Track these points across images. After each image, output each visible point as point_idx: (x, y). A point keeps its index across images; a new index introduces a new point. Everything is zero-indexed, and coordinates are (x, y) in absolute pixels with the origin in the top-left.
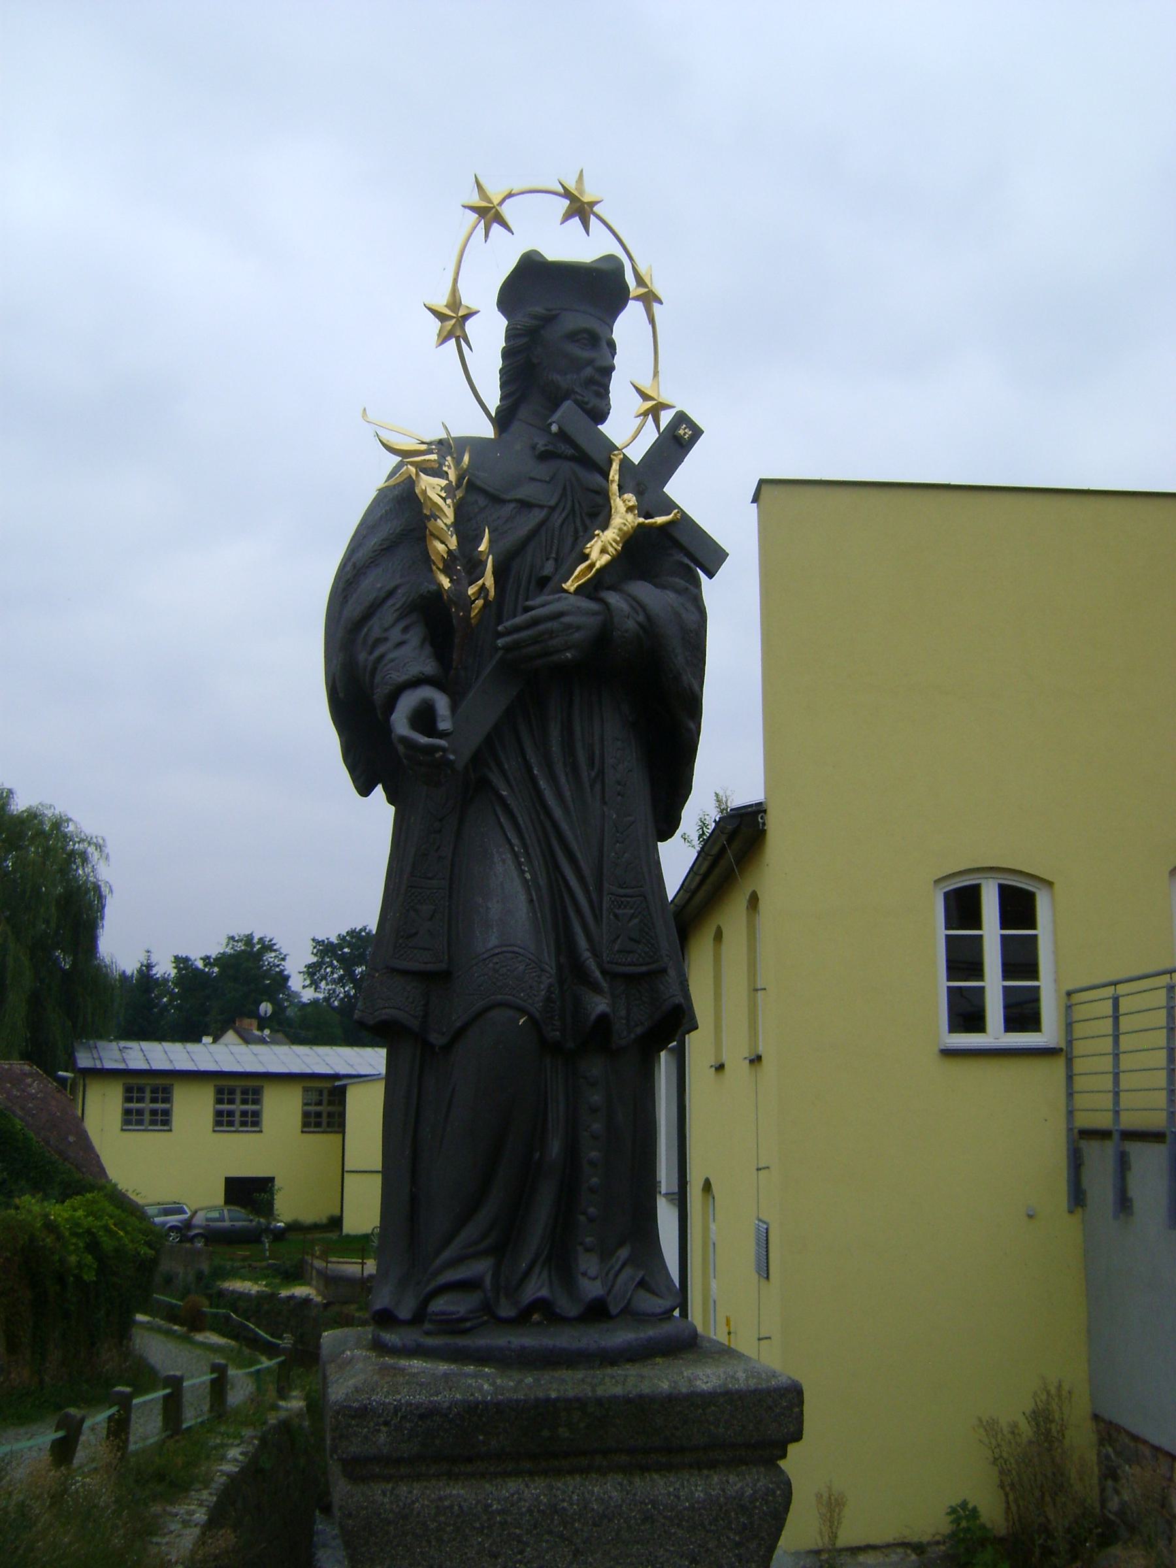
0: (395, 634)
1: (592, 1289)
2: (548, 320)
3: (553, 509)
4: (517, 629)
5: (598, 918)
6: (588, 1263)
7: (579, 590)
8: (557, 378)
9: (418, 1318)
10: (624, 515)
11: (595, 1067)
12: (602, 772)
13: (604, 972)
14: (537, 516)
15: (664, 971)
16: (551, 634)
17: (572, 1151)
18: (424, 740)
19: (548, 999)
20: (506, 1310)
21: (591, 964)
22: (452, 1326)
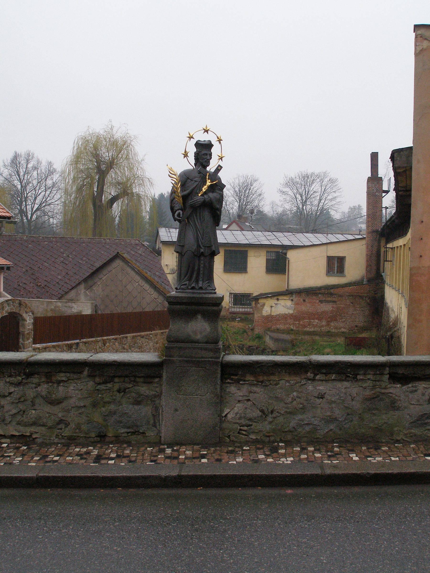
1: (200, 285)
5: (203, 239)
6: (201, 283)
10: (208, 183)
13: (203, 246)
14: (197, 183)
15: (212, 246)
17: (199, 269)
19: (195, 250)
21: (201, 245)
22: (183, 289)
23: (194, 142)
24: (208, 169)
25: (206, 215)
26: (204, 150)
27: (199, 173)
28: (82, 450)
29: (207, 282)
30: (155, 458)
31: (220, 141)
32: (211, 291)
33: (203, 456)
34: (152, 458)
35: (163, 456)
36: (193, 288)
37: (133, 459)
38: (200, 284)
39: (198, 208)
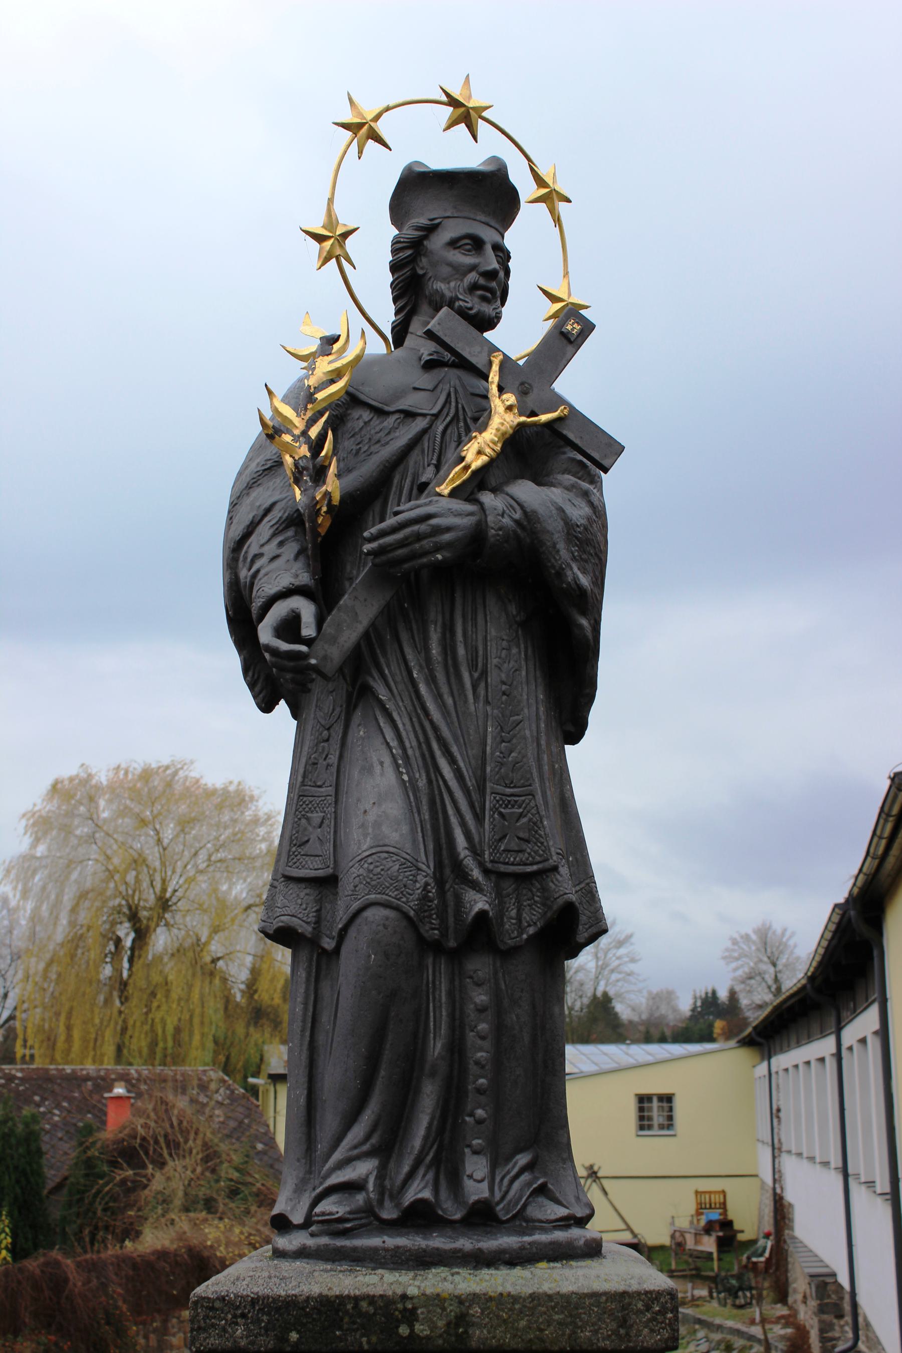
0: (271, 549)
1: (476, 1190)
2: (431, 229)
3: (436, 416)
4: (383, 534)
5: (479, 818)
6: (476, 1167)
7: (454, 494)
10: (503, 416)
11: (480, 966)
12: (484, 673)
13: (486, 872)
14: (420, 424)
15: (555, 869)
16: (419, 537)
17: (457, 1048)
18: (285, 646)
19: (425, 898)
20: (389, 1213)
21: (469, 862)
22: (335, 1227)
25: (494, 637)
26: (453, 227)
29: (523, 1159)
32: (559, 1235)
36: (420, 1217)
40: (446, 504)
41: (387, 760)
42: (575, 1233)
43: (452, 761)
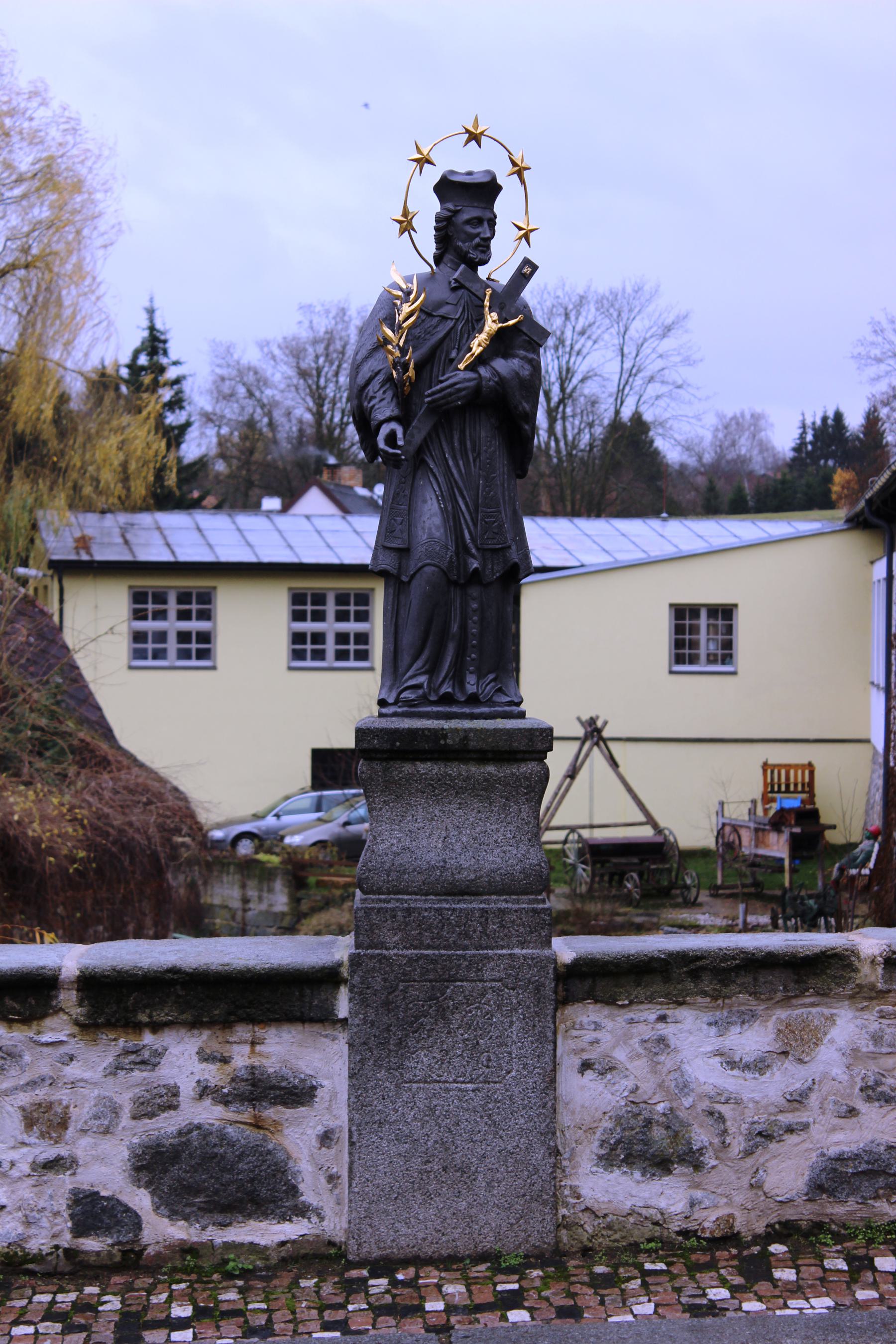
0: (380, 394)
1: (471, 689)
2: (456, 213)
3: (457, 320)
4: (433, 394)
5: (475, 525)
6: (471, 679)
7: (466, 368)
8: (460, 244)
9: (396, 703)
10: (491, 323)
11: (474, 591)
12: (479, 454)
13: (478, 549)
14: (450, 324)
15: (509, 547)
16: (450, 394)
17: (463, 627)
18: (391, 451)
19: (451, 562)
21: (471, 546)
22: (409, 703)
23: (433, 175)
24: (483, 272)
26: (467, 205)
27: (454, 289)
28: (60, 1297)
29: (491, 676)
30: (340, 1315)
31: (519, 172)
32: (507, 708)
33: (513, 1300)
34: (328, 1315)
35: (365, 1306)
36: (447, 699)
37: (262, 1320)
38: (471, 685)
39: (453, 414)
40: (462, 375)
41: (434, 497)
42: (514, 708)
43: (464, 498)
